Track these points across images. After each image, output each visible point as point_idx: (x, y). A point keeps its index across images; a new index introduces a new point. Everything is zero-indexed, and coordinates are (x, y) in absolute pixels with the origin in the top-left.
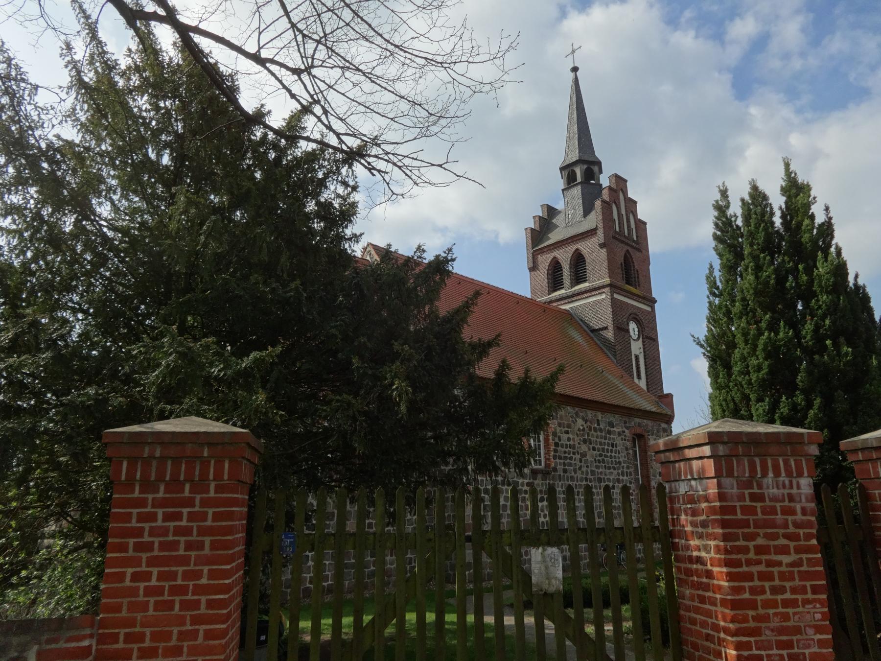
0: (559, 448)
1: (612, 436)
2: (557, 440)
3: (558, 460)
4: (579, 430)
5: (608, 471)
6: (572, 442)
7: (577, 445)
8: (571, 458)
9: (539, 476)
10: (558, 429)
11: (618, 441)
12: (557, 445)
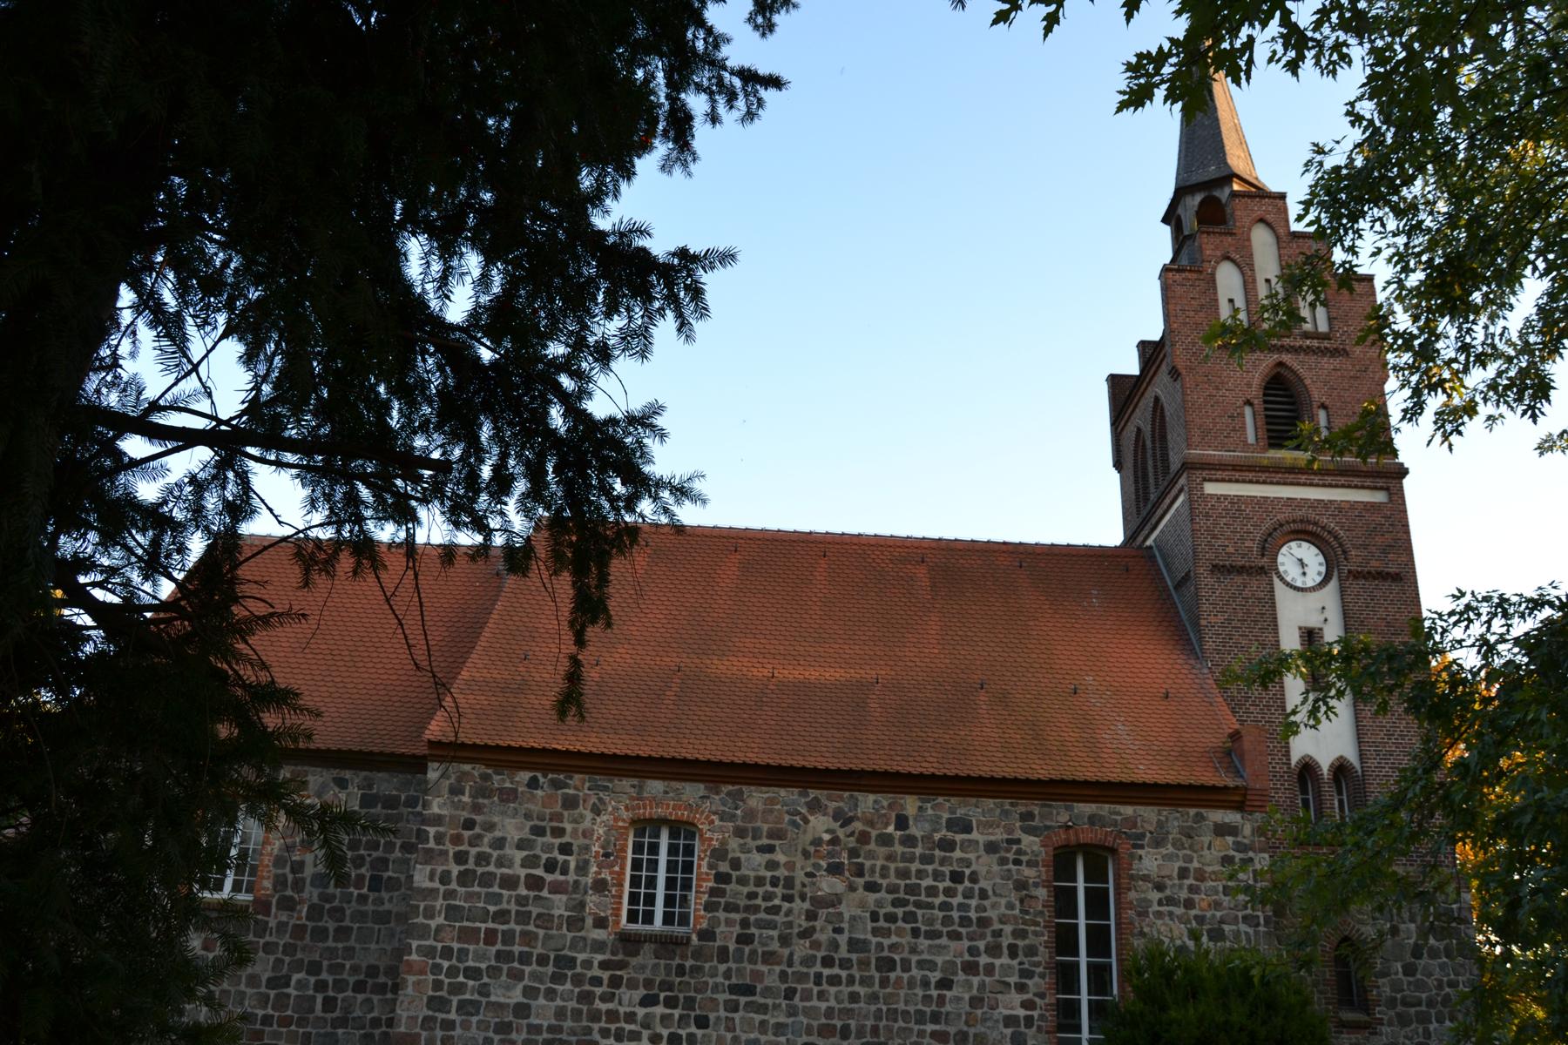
0: (731, 887)
1: (958, 854)
2: (724, 867)
3: (722, 915)
4: (817, 842)
5: (924, 943)
6: (782, 873)
7: (800, 876)
8: (775, 910)
9: (648, 948)
10: (734, 843)
11: (984, 864)
12: (722, 878)
